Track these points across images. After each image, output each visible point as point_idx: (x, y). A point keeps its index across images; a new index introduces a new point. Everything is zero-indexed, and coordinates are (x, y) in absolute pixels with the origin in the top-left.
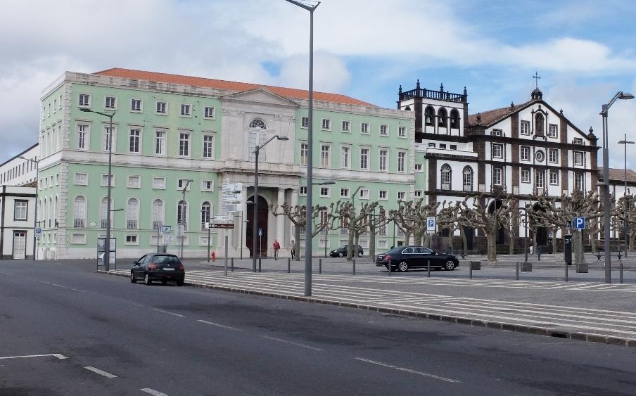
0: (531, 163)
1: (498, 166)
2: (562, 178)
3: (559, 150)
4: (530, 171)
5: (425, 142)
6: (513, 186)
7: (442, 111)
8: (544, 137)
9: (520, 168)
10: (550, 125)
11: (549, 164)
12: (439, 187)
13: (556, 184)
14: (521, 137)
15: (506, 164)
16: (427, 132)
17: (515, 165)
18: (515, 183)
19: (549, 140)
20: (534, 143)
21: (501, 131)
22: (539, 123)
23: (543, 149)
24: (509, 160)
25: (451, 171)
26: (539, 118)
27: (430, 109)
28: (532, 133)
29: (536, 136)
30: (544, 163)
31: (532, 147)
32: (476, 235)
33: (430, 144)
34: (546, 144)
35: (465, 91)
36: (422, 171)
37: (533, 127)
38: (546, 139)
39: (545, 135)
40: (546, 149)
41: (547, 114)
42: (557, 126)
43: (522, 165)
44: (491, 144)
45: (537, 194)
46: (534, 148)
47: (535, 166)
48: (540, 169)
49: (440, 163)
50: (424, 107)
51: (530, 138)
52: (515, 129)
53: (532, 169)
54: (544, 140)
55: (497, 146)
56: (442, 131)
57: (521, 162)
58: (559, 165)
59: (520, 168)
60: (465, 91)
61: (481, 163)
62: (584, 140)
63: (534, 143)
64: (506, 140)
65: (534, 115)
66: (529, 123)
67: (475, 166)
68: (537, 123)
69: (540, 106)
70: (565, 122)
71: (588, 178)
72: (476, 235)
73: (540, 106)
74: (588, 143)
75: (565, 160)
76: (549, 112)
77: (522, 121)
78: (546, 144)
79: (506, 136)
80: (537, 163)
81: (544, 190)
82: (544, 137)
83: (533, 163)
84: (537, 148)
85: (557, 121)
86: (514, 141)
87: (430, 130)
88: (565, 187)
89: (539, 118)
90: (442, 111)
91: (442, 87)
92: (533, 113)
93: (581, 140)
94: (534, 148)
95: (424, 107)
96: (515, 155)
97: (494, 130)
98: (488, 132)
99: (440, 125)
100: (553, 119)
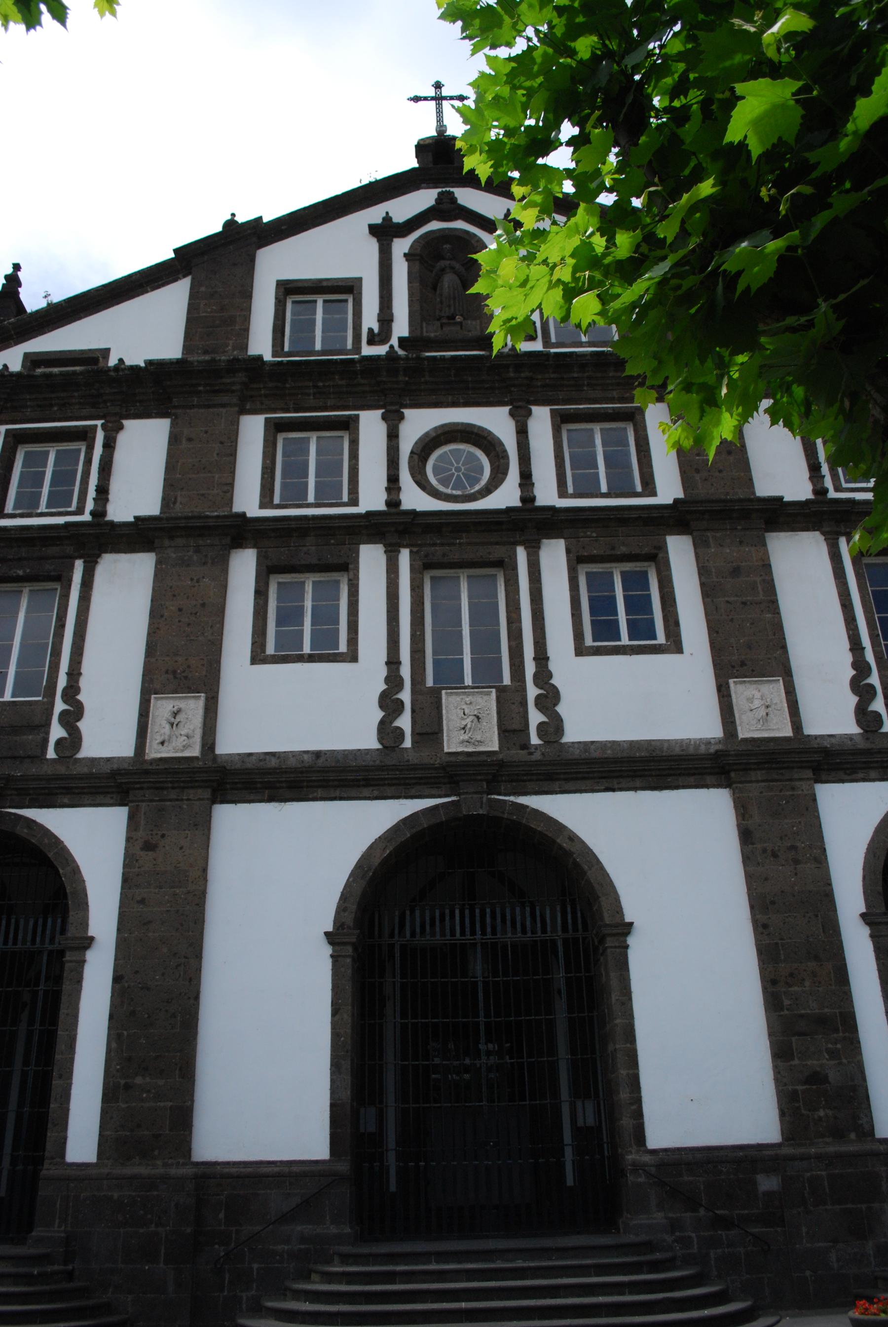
2: (709, 591)
4: (347, 566)
6: (151, 687)
17: (190, 535)
23: (496, 420)
31: (371, 424)
45: (429, 730)
46: (393, 421)
48: (459, 546)
53: (371, 559)
59: (244, 566)
65: (401, 246)
66: (350, 288)
81: (510, 704)
92: (385, 232)
94: (393, 421)
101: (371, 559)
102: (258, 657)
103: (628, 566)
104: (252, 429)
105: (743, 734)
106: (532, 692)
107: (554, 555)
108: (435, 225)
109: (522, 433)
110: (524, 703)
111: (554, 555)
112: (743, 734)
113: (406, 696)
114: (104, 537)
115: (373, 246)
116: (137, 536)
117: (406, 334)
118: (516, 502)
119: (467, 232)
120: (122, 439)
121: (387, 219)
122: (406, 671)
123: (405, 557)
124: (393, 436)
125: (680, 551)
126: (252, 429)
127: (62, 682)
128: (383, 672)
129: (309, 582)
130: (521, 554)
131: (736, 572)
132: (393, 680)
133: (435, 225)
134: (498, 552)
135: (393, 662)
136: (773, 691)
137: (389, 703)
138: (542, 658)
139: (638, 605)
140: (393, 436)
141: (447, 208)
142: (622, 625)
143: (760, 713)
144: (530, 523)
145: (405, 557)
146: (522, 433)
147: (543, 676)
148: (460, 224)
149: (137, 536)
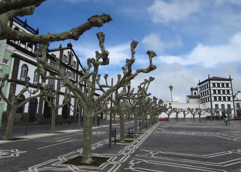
12: (19, 78)
22: (70, 59)
25: (28, 70)
32: (37, 113)
36: (8, 64)
40: (72, 72)
55: (53, 63)
65: (69, 54)
70: (79, 62)
72: (37, 113)
76: (74, 55)
89: (70, 57)
92: (68, 52)
94: (67, 70)
100: (74, 59)
121: (69, 51)
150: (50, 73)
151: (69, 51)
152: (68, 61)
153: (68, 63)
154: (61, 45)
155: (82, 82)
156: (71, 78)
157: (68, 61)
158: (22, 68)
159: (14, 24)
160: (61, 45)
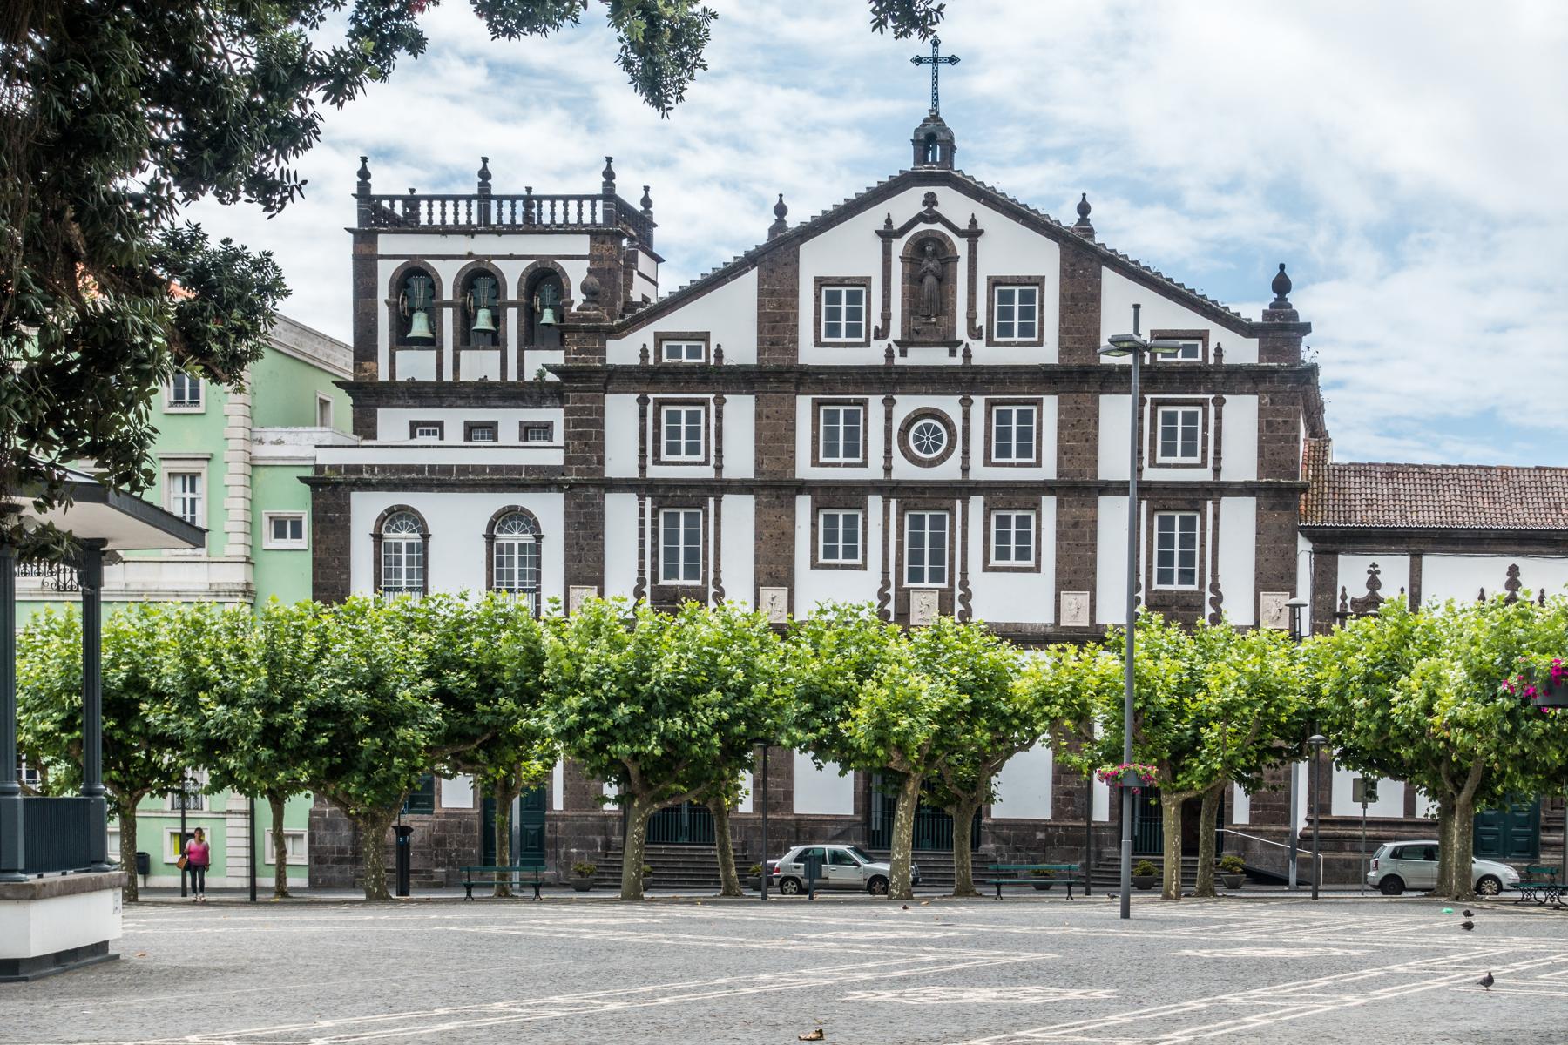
0: (874, 472)
1: (679, 502)
2: (1060, 536)
3: (1050, 404)
4: (863, 507)
5: (393, 422)
6: (758, 585)
7: (480, 279)
8: (953, 346)
9: (804, 504)
10: (994, 282)
11: (979, 472)
13: (1031, 563)
14: (809, 355)
15: (721, 487)
16: (401, 377)
18: (774, 569)
19: (983, 355)
20: (890, 380)
21: (704, 337)
22: (930, 280)
23: (950, 405)
24: (740, 461)
25: (426, 537)
26: (929, 263)
27: (414, 275)
28: (882, 333)
29: (904, 345)
30: (949, 470)
31: (876, 403)
33: (414, 425)
34: (966, 380)
35: (609, 175)
37: (888, 304)
38: (967, 354)
39: (962, 332)
40: (966, 404)
41: (973, 234)
42: (1039, 282)
43: (803, 487)
44: (643, 402)
46: (889, 403)
47: (888, 488)
49: (366, 509)
50: (386, 271)
51: (874, 355)
52: (776, 320)
53: (875, 502)
54: (958, 360)
55: (683, 410)
56: (480, 365)
57: (804, 470)
58: (1048, 470)
59: (804, 504)
60: (609, 175)
61: (584, 488)
62: (1219, 335)
63: (890, 380)
64: (723, 379)
65: (898, 246)
66: (865, 282)
67: (549, 509)
68: (914, 279)
69: (931, 200)
70: (1083, 256)
71: (1237, 528)
73: (931, 200)
74: (1242, 351)
75: (1080, 435)
76: (988, 218)
77: (820, 282)
78: (966, 380)
79: (730, 359)
80: (904, 470)
82: (953, 346)
83: (881, 476)
84: (906, 405)
85: (1041, 260)
86: (774, 378)
87: (416, 366)
88: (1077, 571)
89: (929, 263)
90: (479, 277)
91: (485, 175)
93: (1203, 336)
94: (889, 403)
95: (386, 271)
96: (774, 438)
97: (660, 338)
98: (623, 351)
99: (467, 338)
101: (875, 502)
102: (814, 565)
103: (1020, 513)
104: (804, 404)
105: (1063, 624)
106: (958, 592)
107: (977, 504)
108: (922, 227)
109: (966, 417)
110: (952, 599)
111: (977, 504)
112: (1063, 624)
113: (891, 592)
114: (721, 487)
115: (878, 244)
116: (742, 487)
117: (899, 338)
118: (958, 476)
119: (943, 235)
120: (726, 408)
121: (889, 222)
122: (892, 578)
123: (893, 502)
124: (888, 418)
125: (1049, 504)
126: (804, 404)
127: (711, 576)
128: (880, 578)
129: (841, 514)
130: (958, 502)
131: (1076, 525)
132: (886, 583)
133: (922, 227)
134: (946, 503)
135: (885, 573)
136: (1084, 598)
137: (884, 597)
138: (964, 573)
139: (1023, 537)
140: (888, 418)
141: (931, 216)
142: (1011, 549)
143: (1075, 611)
144: (964, 489)
145: (893, 502)
146: (966, 417)
147: (964, 584)
148: (938, 227)
149: (742, 487)
150: (641, 497)
151: (889, 222)
152: (886, 317)
153: (896, 332)
154: (781, 210)
155: (1205, 452)
156: (965, 470)
157: (886, 317)
158: (377, 537)
159: (383, 257)
160: (781, 210)
